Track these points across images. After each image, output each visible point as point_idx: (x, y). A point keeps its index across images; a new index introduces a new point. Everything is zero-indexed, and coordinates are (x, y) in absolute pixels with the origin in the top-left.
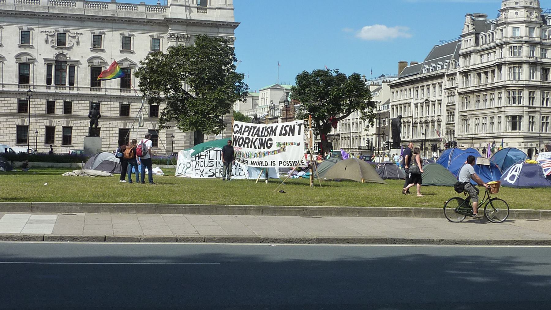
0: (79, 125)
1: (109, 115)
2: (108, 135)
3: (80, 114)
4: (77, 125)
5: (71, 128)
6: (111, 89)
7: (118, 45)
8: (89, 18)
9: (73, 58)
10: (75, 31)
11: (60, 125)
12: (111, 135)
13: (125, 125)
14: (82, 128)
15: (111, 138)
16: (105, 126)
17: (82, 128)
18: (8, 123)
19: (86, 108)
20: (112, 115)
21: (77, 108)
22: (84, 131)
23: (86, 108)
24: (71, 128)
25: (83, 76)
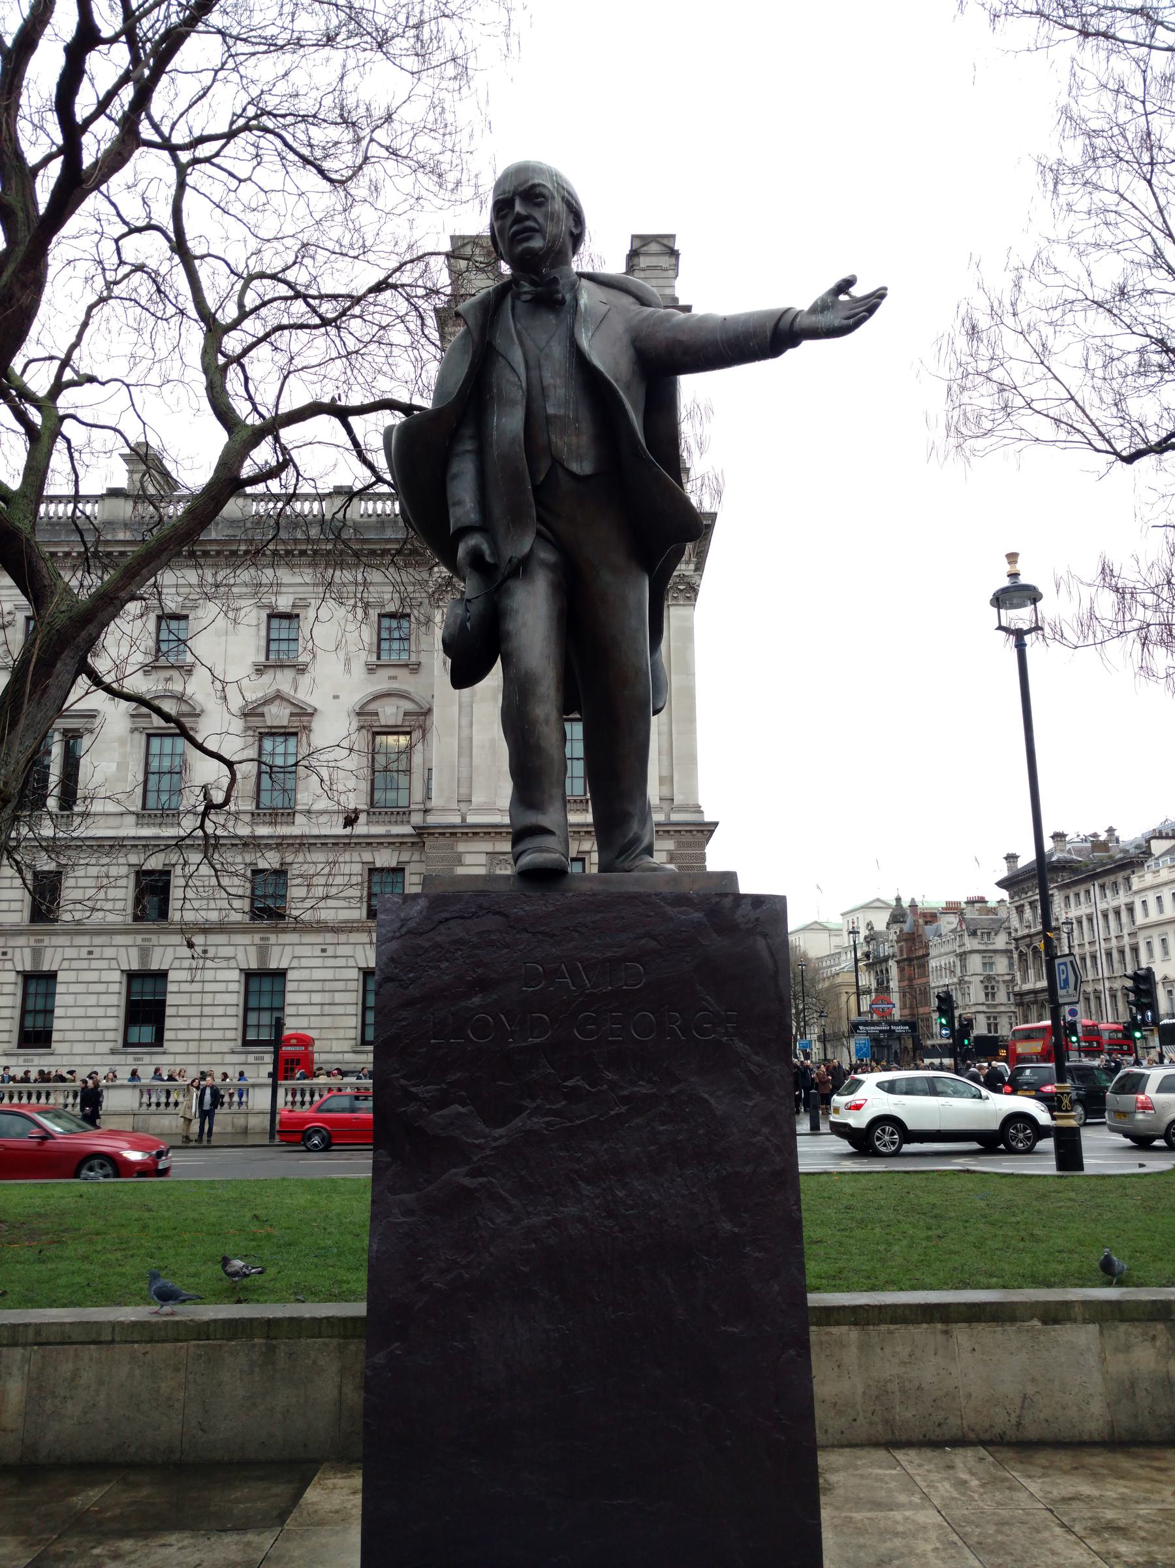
0: (84, 964)
4: (76, 964)
5: (52, 976)
11: (9, 965)
12: (208, 999)
13: (263, 951)
14: (93, 976)
15: (207, 1011)
17: (93, 976)
22: (101, 988)
24: (52, 976)
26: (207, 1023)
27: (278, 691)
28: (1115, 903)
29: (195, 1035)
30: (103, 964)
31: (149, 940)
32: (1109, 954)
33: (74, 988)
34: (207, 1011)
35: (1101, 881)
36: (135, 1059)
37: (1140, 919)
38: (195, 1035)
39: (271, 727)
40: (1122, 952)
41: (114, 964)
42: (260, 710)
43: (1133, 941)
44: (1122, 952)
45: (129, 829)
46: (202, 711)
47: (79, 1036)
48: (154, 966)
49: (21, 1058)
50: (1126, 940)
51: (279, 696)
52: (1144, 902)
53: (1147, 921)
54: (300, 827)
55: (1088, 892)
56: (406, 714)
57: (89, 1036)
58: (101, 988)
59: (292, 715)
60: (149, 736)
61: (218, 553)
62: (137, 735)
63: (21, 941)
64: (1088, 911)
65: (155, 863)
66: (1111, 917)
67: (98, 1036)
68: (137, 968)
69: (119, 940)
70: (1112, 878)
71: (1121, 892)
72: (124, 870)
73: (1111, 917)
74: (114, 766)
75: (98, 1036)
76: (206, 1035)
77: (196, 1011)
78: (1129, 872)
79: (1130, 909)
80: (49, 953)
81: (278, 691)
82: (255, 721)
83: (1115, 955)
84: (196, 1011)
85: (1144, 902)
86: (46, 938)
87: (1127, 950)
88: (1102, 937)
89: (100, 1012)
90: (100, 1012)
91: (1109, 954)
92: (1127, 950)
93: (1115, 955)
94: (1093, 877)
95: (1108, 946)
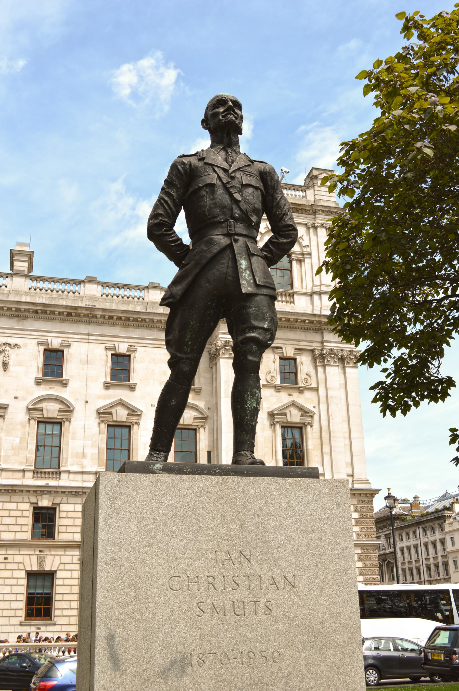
6: (83, 473)
7: (102, 369)
8: (36, 312)
16: (68, 567)
18: (9, 566)
19: (21, 521)
22: (14, 582)
23: (21, 521)
27: (121, 400)
28: (433, 539)
30: (15, 566)
31: (44, 551)
32: (428, 567)
35: (423, 526)
37: (449, 547)
39: (116, 421)
40: (437, 566)
41: (21, 566)
42: (109, 411)
43: (444, 560)
44: (437, 566)
45: (29, 480)
46: (74, 409)
48: (47, 568)
50: (440, 560)
51: (121, 403)
52: (452, 538)
53: (454, 548)
54: (65, 481)
55: (415, 532)
56: (195, 418)
58: (14, 582)
59: (129, 415)
60: (39, 422)
61: (103, 317)
62: (32, 422)
64: (415, 543)
65: (45, 502)
66: (430, 547)
67: (12, 613)
68: (36, 569)
70: (431, 524)
71: (437, 532)
72: (26, 506)
73: (430, 547)
74: (18, 440)
75: (12, 613)
78: (442, 521)
79: (443, 542)
82: (107, 418)
83: (433, 568)
85: (452, 538)
87: (440, 564)
88: (424, 557)
89: (13, 597)
90: (13, 597)
91: (428, 567)
92: (440, 564)
93: (433, 568)
94: (418, 524)
95: (428, 563)
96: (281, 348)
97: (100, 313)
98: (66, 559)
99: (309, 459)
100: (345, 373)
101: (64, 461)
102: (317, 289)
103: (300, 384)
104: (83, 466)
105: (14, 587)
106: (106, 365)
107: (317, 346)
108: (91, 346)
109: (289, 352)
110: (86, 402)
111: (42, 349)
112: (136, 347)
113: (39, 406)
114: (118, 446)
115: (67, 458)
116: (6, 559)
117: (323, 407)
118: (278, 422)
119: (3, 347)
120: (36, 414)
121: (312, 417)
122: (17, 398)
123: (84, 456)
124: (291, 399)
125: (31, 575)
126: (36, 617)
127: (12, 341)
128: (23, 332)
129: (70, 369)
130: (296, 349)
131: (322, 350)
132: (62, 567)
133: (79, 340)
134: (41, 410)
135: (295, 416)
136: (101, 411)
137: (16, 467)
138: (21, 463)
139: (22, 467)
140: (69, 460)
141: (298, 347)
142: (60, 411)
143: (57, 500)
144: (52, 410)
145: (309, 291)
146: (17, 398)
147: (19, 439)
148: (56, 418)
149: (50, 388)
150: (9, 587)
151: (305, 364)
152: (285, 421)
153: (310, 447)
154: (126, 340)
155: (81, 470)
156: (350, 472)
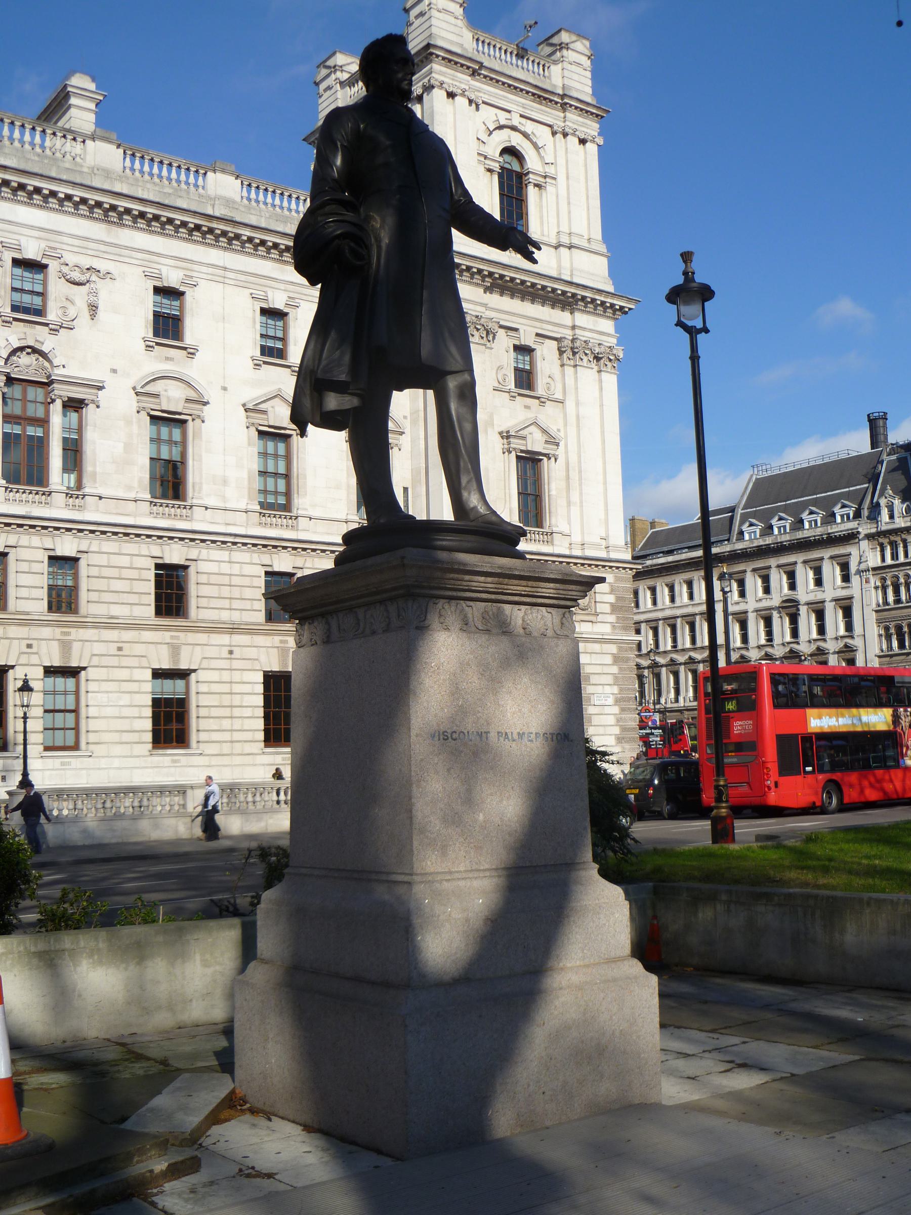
0: (114, 661)
1: (225, 616)
2: (226, 700)
3: (116, 610)
4: (105, 661)
9: (74, 371)
10: (86, 262)
11: (35, 659)
12: (237, 700)
14: (124, 674)
15: (237, 712)
17: (124, 674)
20: (236, 617)
21: (101, 584)
25: (118, 452)
26: (237, 724)
27: (280, 390)
29: (227, 736)
33: (106, 686)
34: (237, 712)
36: (174, 761)
38: (227, 736)
42: (263, 407)
47: (115, 737)
49: (59, 761)
57: (126, 737)
63: (46, 632)
69: (148, 635)
76: (237, 736)
77: (226, 712)
80: (76, 646)
81: (280, 390)
82: (258, 419)
84: (226, 712)
86: (73, 631)
96: (516, 330)
97: (248, 234)
98: (211, 652)
99: (553, 510)
100: (600, 381)
101: (197, 488)
102: (565, 240)
103: (540, 390)
104: (224, 498)
105: (246, 697)
106: (254, 327)
107: (568, 334)
108: (229, 289)
109: (528, 340)
110: (225, 389)
111: (150, 285)
112: (297, 301)
113: (149, 389)
114: (271, 469)
115: (201, 483)
116: (120, 649)
117: (572, 431)
118: (515, 449)
119: (88, 275)
120: (149, 403)
121: (557, 445)
122: (114, 371)
123: (225, 482)
124: (530, 415)
125: (158, 674)
126: (165, 743)
127: (96, 264)
128: (117, 250)
129: (194, 329)
130: (538, 335)
131: (573, 340)
132: (205, 664)
133: (210, 277)
134: (157, 396)
135: (536, 442)
136: (250, 406)
137: (121, 494)
138: (129, 488)
139: (132, 495)
140: (205, 487)
141: (540, 332)
142: (188, 400)
143: (193, 554)
144: (173, 398)
145: (554, 242)
146: (114, 371)
147: (122, 445)
148: (180, 414)
149: (167, 359)
150: (127, 696)
151: (547, 359)
152: (523, 448)
153: (553, 493)
154: (282, 286)
155: (221, 505)
156: (604, 535)
